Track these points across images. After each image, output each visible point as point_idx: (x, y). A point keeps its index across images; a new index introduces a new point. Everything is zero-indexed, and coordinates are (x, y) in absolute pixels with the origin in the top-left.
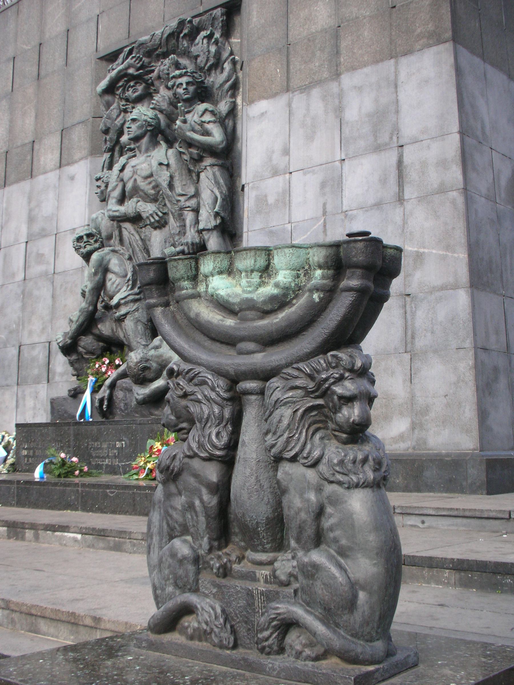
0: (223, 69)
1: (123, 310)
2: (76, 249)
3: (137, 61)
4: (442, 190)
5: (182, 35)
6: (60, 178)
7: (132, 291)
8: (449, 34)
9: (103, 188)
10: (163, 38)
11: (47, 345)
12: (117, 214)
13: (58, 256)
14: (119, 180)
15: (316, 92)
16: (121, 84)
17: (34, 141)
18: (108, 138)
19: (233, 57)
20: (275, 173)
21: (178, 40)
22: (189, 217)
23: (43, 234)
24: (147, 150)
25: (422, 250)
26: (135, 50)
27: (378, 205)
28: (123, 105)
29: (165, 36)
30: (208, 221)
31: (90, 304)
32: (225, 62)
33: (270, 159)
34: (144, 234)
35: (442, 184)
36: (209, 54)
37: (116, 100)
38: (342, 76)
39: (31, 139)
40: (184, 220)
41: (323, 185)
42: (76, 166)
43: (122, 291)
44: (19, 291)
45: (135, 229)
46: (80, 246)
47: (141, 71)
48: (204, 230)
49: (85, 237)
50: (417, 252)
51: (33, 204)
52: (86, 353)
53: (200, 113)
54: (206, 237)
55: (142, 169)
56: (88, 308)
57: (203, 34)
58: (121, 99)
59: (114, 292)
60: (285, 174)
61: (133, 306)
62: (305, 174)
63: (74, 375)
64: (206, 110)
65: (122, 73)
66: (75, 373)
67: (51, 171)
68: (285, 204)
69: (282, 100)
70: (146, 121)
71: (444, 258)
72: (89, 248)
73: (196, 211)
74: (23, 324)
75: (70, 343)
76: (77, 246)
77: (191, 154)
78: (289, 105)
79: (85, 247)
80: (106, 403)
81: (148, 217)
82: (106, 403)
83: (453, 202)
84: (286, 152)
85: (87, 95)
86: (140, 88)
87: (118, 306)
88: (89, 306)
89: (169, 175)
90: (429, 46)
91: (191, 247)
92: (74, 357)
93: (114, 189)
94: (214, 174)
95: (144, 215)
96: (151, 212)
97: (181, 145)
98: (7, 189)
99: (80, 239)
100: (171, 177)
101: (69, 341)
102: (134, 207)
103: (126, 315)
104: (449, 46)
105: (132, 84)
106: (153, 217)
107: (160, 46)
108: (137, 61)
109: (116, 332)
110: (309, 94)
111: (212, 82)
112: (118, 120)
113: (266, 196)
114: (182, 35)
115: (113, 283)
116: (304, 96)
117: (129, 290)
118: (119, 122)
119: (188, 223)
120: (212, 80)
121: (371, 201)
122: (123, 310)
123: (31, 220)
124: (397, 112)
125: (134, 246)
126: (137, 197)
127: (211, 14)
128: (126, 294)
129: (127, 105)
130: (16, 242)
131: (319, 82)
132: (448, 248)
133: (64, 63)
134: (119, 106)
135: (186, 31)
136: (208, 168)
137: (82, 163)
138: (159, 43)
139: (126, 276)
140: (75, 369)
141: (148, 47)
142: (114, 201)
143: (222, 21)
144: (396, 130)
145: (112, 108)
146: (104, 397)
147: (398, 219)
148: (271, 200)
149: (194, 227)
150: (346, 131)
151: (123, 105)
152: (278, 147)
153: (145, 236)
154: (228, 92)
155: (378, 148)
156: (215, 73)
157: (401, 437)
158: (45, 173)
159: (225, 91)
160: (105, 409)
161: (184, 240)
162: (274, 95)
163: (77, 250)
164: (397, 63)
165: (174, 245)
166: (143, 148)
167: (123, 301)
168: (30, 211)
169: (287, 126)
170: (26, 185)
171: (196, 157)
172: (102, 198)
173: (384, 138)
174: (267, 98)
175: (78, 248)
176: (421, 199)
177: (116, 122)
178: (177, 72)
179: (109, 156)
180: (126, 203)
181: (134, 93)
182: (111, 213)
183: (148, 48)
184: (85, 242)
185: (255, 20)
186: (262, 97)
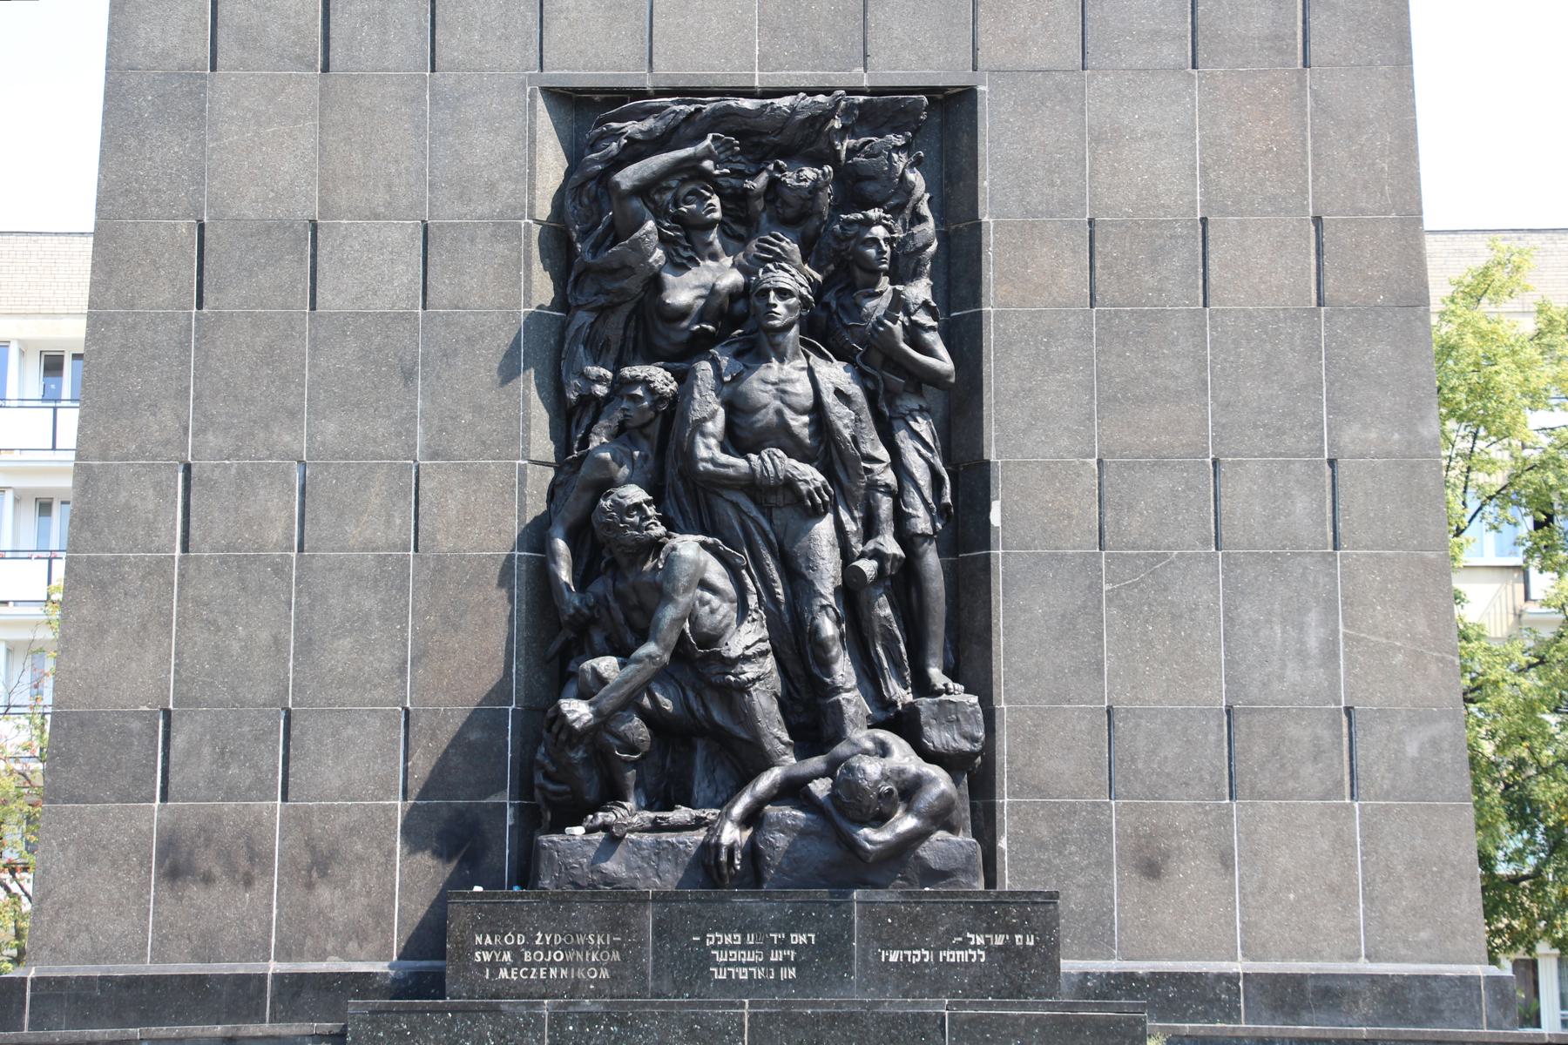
1: (750, 671)
3: (721, 149)
12: (731, 471)
16: (674, 183)
22: (885, 505)
28: (666, 228)
49: (644, 505)
55: (797, 395)
70: (801, 297)
73: (898, 496)
79: (647, 528)
81: (810, 493)
82: (738, 855)
92: (577, 755)
95: (803, 487)
103: (753, 681)
108: (721, 149)
115: (713, 612)
138: (780, 125)
141: (746, 124)
160: (739, 867)
167: (749, 652)
177: (651, 260)
179: (593, 320)
183: (744, 127)
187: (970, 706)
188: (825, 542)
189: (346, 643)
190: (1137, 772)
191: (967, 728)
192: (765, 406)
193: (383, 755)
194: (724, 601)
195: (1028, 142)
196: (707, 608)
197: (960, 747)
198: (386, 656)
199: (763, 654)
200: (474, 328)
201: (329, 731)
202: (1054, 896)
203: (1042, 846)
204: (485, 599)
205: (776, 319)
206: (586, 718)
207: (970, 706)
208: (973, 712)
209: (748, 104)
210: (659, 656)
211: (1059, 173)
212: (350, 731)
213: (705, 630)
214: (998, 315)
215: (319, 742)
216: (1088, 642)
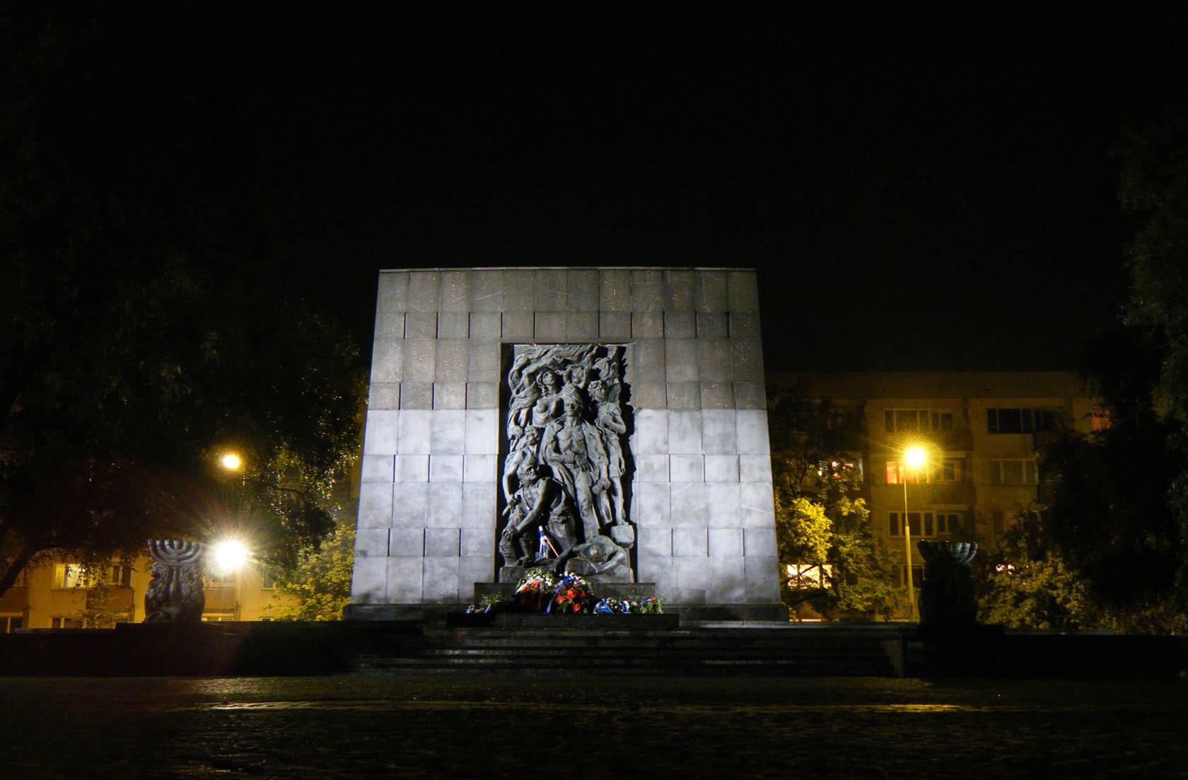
4: (761, 481)
6: (466, 416)
8: (765, 406)
11: (459, 531)
13: (467, 470)
15: (685, 414)
20: (659, 452)
23: (449, 452)
25: (750, 508)
27: (726, 482)
33: (655, 444)
35: (761, 478)
38: (703, 410)
39: (432, 380)
41: (691, 465)
42: (483, 411)
44: (423, 489)
50: (748, 509)
51: (436, 429)
60: (665, 454)
62: (679, 457)
67: (456, 409)
68: (665, 470)
69: (663, 413)
71: (762, 513)
74: (429, 514)
78: (668, 417)
83: (767, 487)
84: (666, 442)
90: (755, 409)
98: (402, 412)
104: (766, 412)
110: (681, 415)
113: (652, 464)
116: (678, 414)
121: (721, 479)
123: (434, 440)
124: (736, 437)
130: (417, 452)
131: (688, 409)
132: (764, 509)
137: (490, 411)
144: (735, 446)
147: (738, 491)
148: (656, 467)
150: (706, 440)
152: (660, 438)
155: (725, 453)
157: (740, 598)
158: (450, 409)
162: (655, 408)
164: (736, 413)
168: (433, 433)
169: (666, 428)
170: (428, 414)
173: (729, 448)
174: (651, 409)
176: (749, 483)
185: (641, 360)
186: (647, 407)
202: (654, 584)
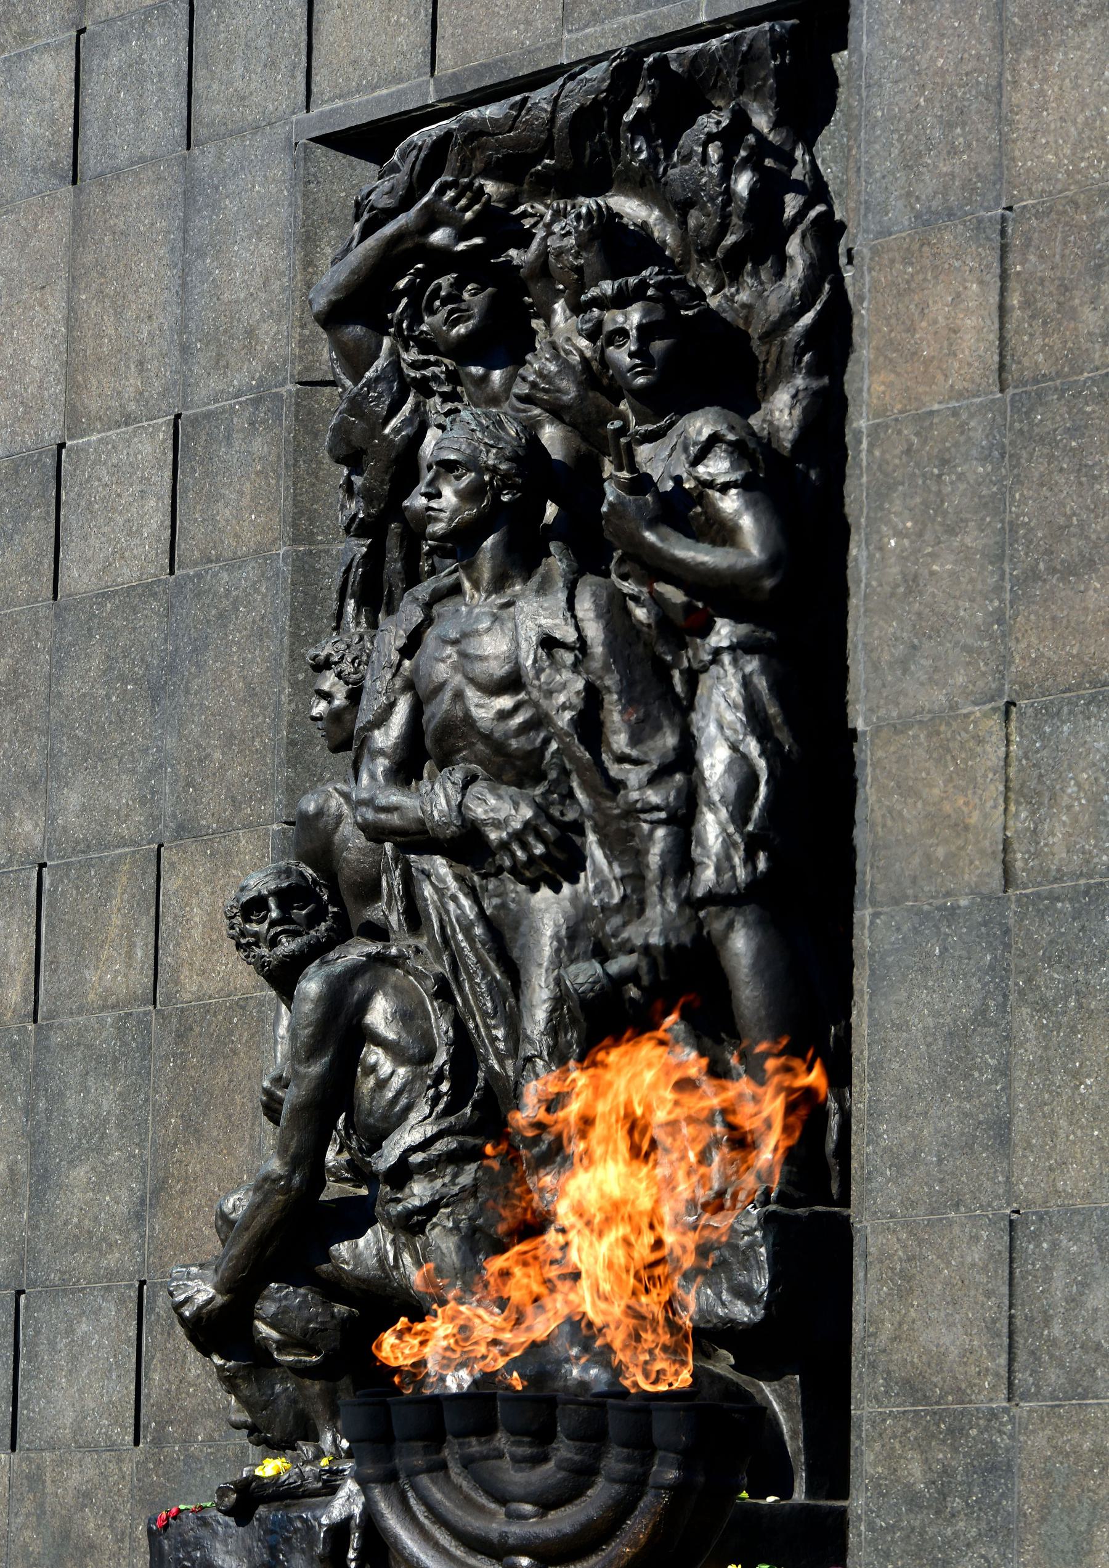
0: (782, 263)
1: (419, 1192)
2: (239, 946)
5: (628, 117)
7: (452, 1119)
9: (339, 701)
10: (559, 123)
12: (395, 819)
14: (398, 683)
16: (401, 284)
17: (62, 446)
18: (358, 481)
19: (820, 208)
21: (615, 134)
24: (499, 583)
26: (453, 158)
29: (563, 116)
30: (724, 864)
31: (294, 1164)
32: (792, 230)
34: (496, 901)
36: (727, 202)
37: (386, 342)
40: (639, 855)
43: (414, 1117)
45: (459, 878)
46: (256, 934)
47: (478, 241)
48: (711, 898)
52: (282, 1347)
53: (693, 450)
54: (717, 926)
56: (289, 1177)
57: (707, 123)
58: (404, 341)
59: (385, 1117)
61: (455, 1176)
63: (237, 1426)
64: (714, 439)
65: (409, 244)
66: (244, 1417)
72: (288, 946)
75: (223, 1307)
76: (243, 934)
77: (657, 600)
80: (355, 1540)
81: (504, 846)
82: (355, 1540)
85: (276, 286)
86: (473, 298)
87: (401, 1174)
88: (292, 1172)
89: (580, 684)
91: (661, 961)
93: (382, 719)
94: (746, 683)
96: (517, 825)
97: (626, 569)
99: (253, 907)
100: (593, 695)
101: (220, 1300)
102: (454, 803)
103: (431, 1209)
105: (445, 282)
106: (525, 846)
107: (547, 148)
109: (396, 1266)
111: (744, 306)
112: (394, 422)
114: (628, 117)
115: (382, 1084)
117: (439, 1117)
118: (397, 431)
119: (654, 857)
120: (744, 297)
122: (419, 1192)
125: (457, 944)
126: (465, 760)
127: (736, 41)
128: (430, 1130)
129: (426, 364)
133: (179, 131)
134: (401, 370)
135: (640, 103)
136: (726, 658)
139: (429, 1057)
140: (246, 1403)
142: (381, 765)
143: (778, 72)
145: (370, 374)
146: (350, 1517)
149: (676, 885)
151: (414, 365)
153: (503, 906)
154: (800, 352)
156: (755, 274)
159: (790, 349)
161: (634, 933)
163: (244, 944)
165: (601, 953)
166: (486, 575)
167: (417, 1158)
171: (679, 619)
172: (340, 736)
175: (249, 944)
177: (387, 431)
178: (607, 287)
180: (425, 786)
181: (455, 323)
182: (370, 815)
184: (273, 924)
187: (746, 1233)
188: (548, 932)
189: (81, 1173)
190: (1053, 1342)
191: (743, 1277)
192: (441, 686)
193: (118, 1366)
194: (402, 1064)
195: (919, 73)
196: (371, 1082)
197: (732, 1316)
198: (124, 1194)
199: (457, 1158)
200: (228, 592)
201: (62, 1327)
203: (913, 1500)
204: (231, 1081)
205: (437, 520)
206: (201, 1298)
207: (746, 1233)
208: (752, 1246)
209: (491, 111)
210: (281, 1177)
211: (964, 124)
212: (84, 1327)
213: (371, 1121)
214: (874, 430)
215: (52, 1344)
216: (989, 1082)
